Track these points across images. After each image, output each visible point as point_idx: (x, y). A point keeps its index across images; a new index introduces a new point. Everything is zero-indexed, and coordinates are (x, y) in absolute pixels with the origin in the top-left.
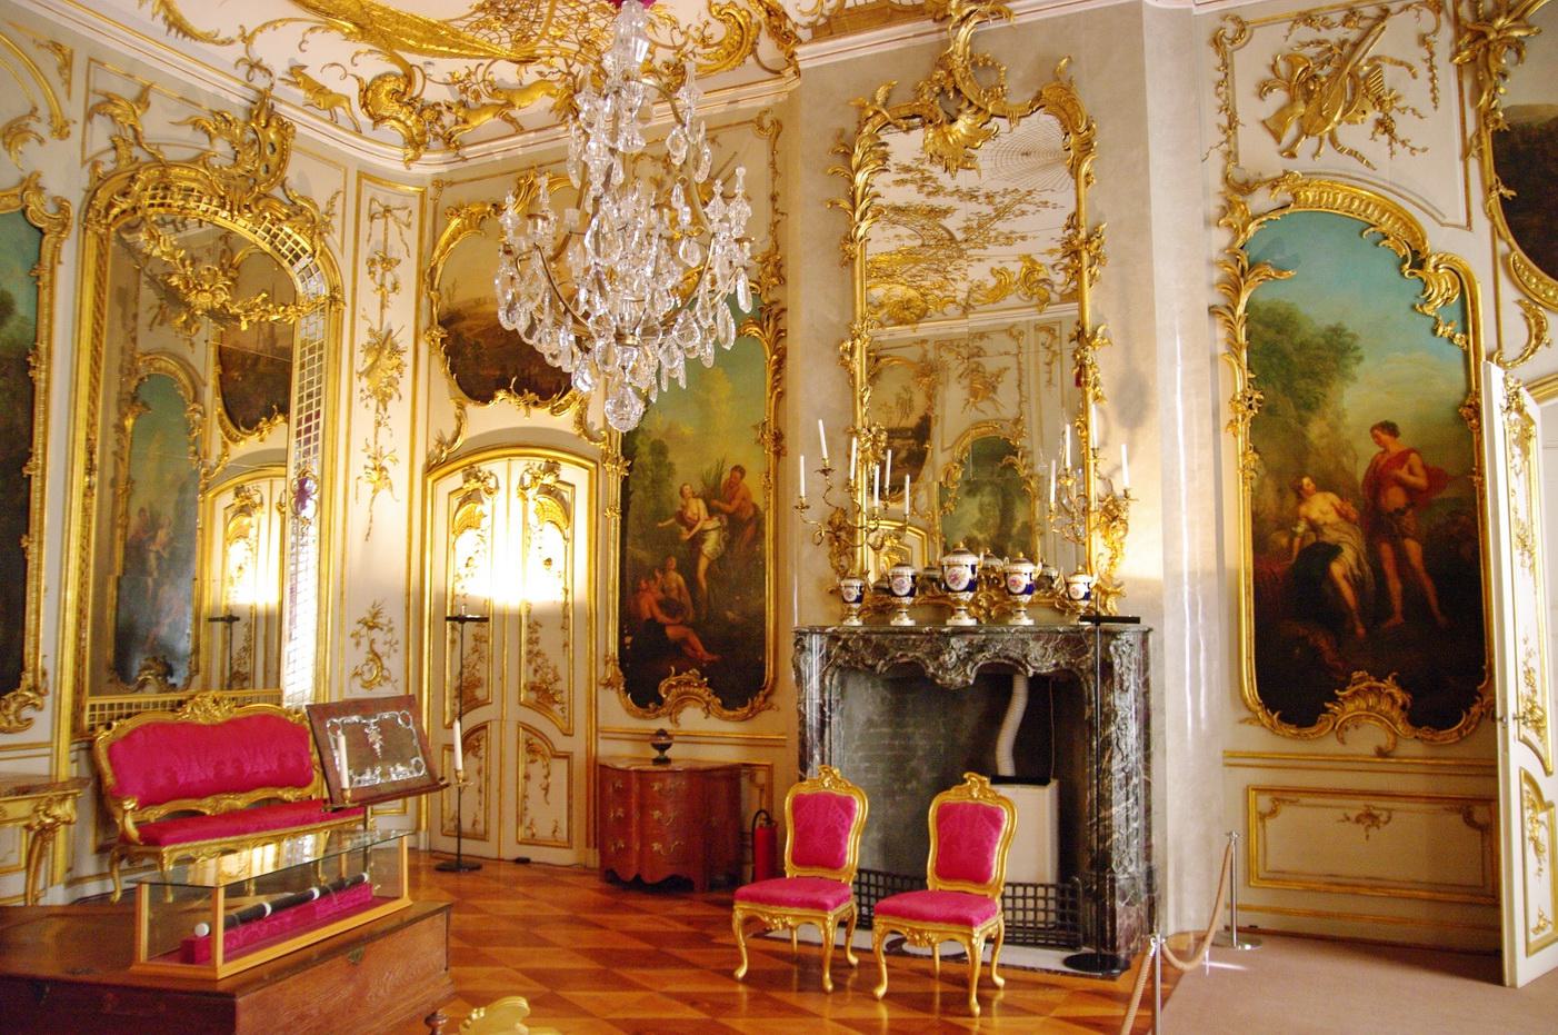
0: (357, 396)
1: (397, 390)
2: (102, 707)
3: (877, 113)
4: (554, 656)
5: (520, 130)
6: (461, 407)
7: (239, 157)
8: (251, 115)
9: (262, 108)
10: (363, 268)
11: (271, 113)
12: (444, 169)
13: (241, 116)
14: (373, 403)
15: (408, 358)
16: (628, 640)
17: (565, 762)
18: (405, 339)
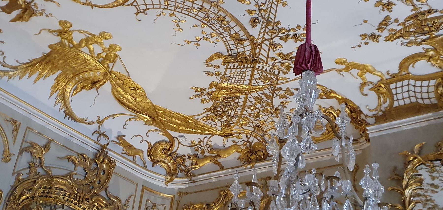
7: (87, 175)
9: (102, 152)
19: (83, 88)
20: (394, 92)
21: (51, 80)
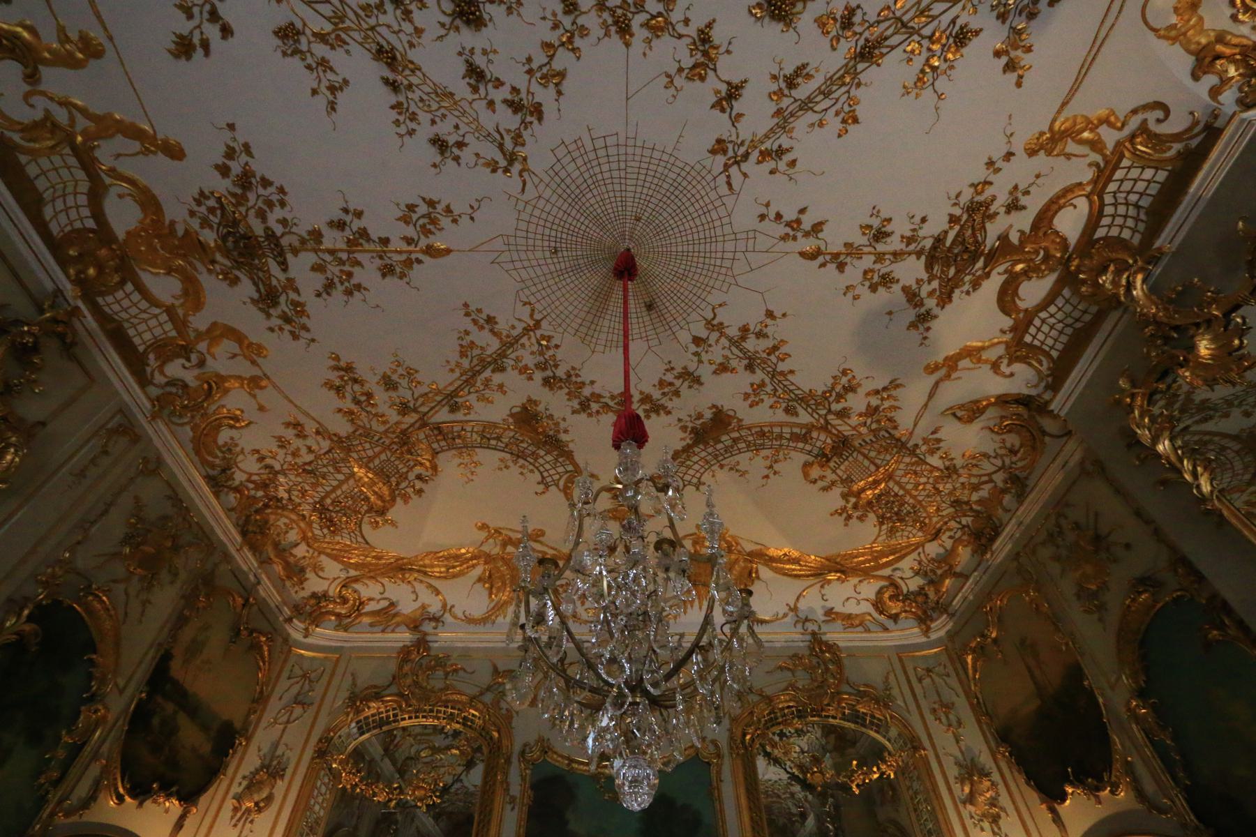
3: (1133, 396)
5: (967, 578)
8: (812, 649)
10: (930, 718)
11: (821, 642)
12: (949, 627)
13: (807, 653)
18: (985, 759)
20: (1036, 343)
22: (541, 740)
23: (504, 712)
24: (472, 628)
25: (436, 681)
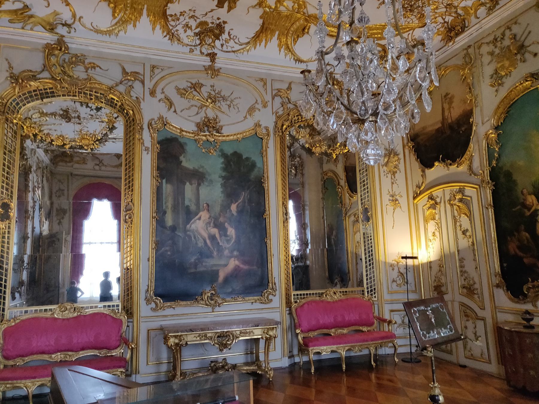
0: (382, 174)
1: (398, 169)
2: (297, 295)
4: (473, 274)
6: (423, 171)
14: (389, 175)
15: (401, 156)
16: (505, 265)
17: (483, 322)
19: (298, 37)
21: (275, 41)
22: (161, 118)
23: (134, 98)
24: (100, 37)
25: (79, 72)
